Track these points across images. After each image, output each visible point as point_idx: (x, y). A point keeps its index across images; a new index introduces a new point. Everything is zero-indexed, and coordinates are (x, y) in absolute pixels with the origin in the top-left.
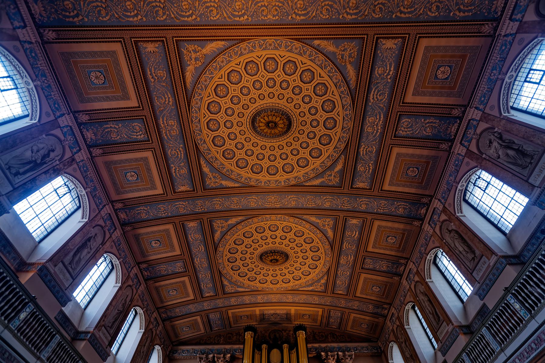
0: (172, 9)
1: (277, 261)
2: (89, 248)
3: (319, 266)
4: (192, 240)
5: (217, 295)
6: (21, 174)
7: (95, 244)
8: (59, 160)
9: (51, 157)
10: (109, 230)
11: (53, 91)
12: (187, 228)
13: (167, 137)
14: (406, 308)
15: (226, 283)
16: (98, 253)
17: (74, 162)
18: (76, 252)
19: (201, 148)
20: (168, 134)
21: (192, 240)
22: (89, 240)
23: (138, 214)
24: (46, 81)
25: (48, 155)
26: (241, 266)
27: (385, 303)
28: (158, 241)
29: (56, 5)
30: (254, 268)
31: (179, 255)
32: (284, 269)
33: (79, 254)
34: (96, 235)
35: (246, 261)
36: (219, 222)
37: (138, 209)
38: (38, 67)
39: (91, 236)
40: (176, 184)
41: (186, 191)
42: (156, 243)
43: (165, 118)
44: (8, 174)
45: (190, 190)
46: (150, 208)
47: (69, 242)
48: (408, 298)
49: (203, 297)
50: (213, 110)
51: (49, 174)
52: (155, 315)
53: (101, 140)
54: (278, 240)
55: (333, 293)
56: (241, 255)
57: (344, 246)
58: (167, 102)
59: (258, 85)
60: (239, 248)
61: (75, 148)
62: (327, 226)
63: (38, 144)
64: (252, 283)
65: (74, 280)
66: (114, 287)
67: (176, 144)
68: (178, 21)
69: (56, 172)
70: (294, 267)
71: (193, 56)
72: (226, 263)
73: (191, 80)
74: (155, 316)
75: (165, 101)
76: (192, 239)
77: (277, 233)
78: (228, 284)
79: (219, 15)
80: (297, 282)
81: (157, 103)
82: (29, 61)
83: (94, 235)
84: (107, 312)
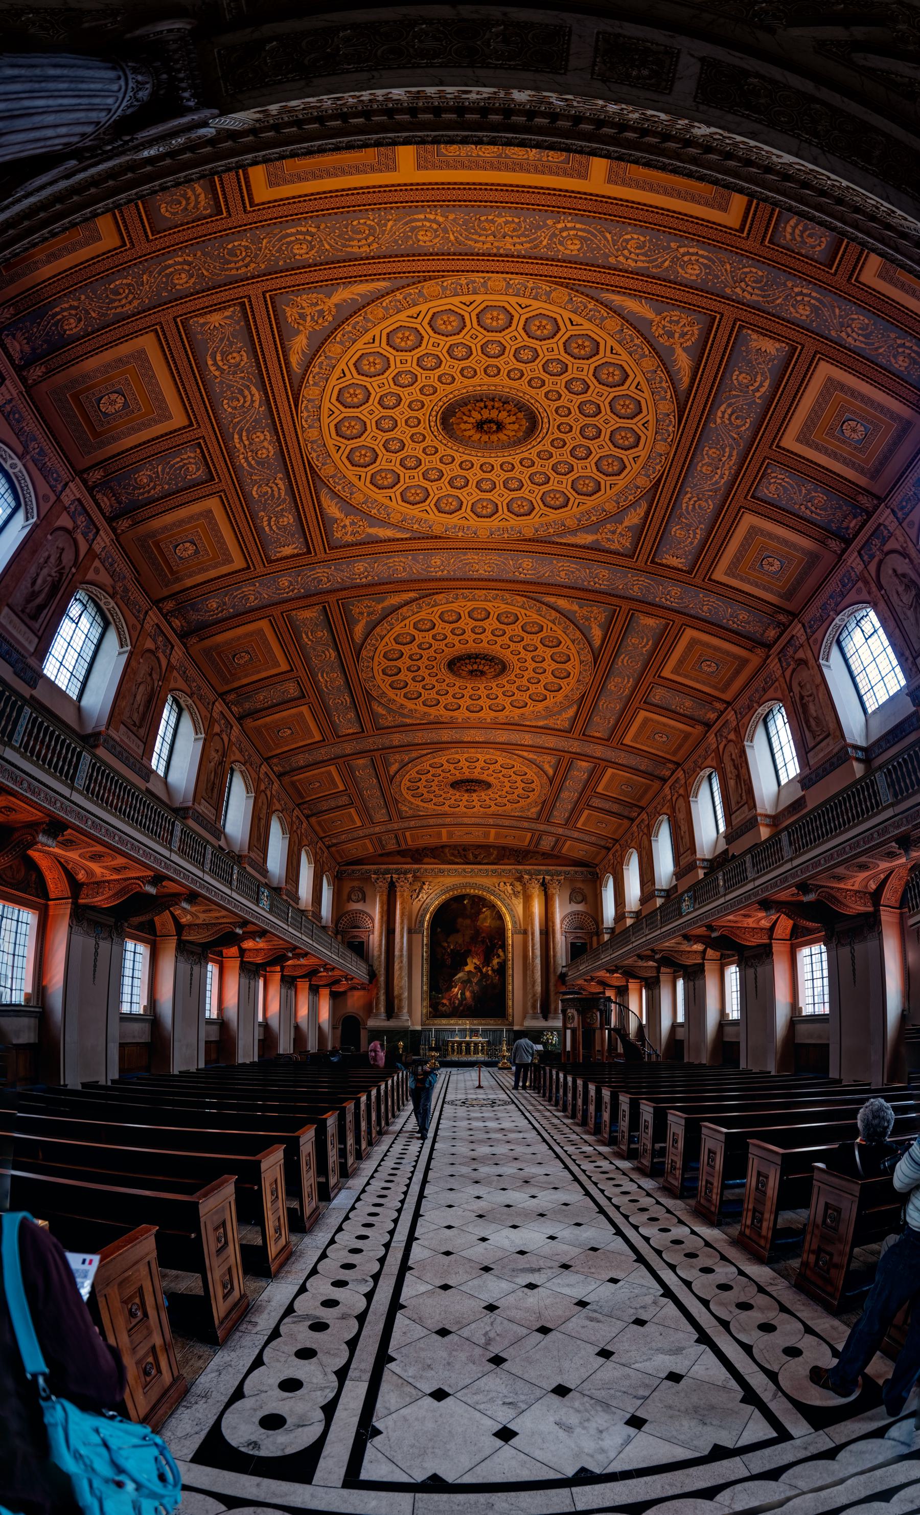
48: (709, 762)
49: (339, 737)
59: (460, 352)
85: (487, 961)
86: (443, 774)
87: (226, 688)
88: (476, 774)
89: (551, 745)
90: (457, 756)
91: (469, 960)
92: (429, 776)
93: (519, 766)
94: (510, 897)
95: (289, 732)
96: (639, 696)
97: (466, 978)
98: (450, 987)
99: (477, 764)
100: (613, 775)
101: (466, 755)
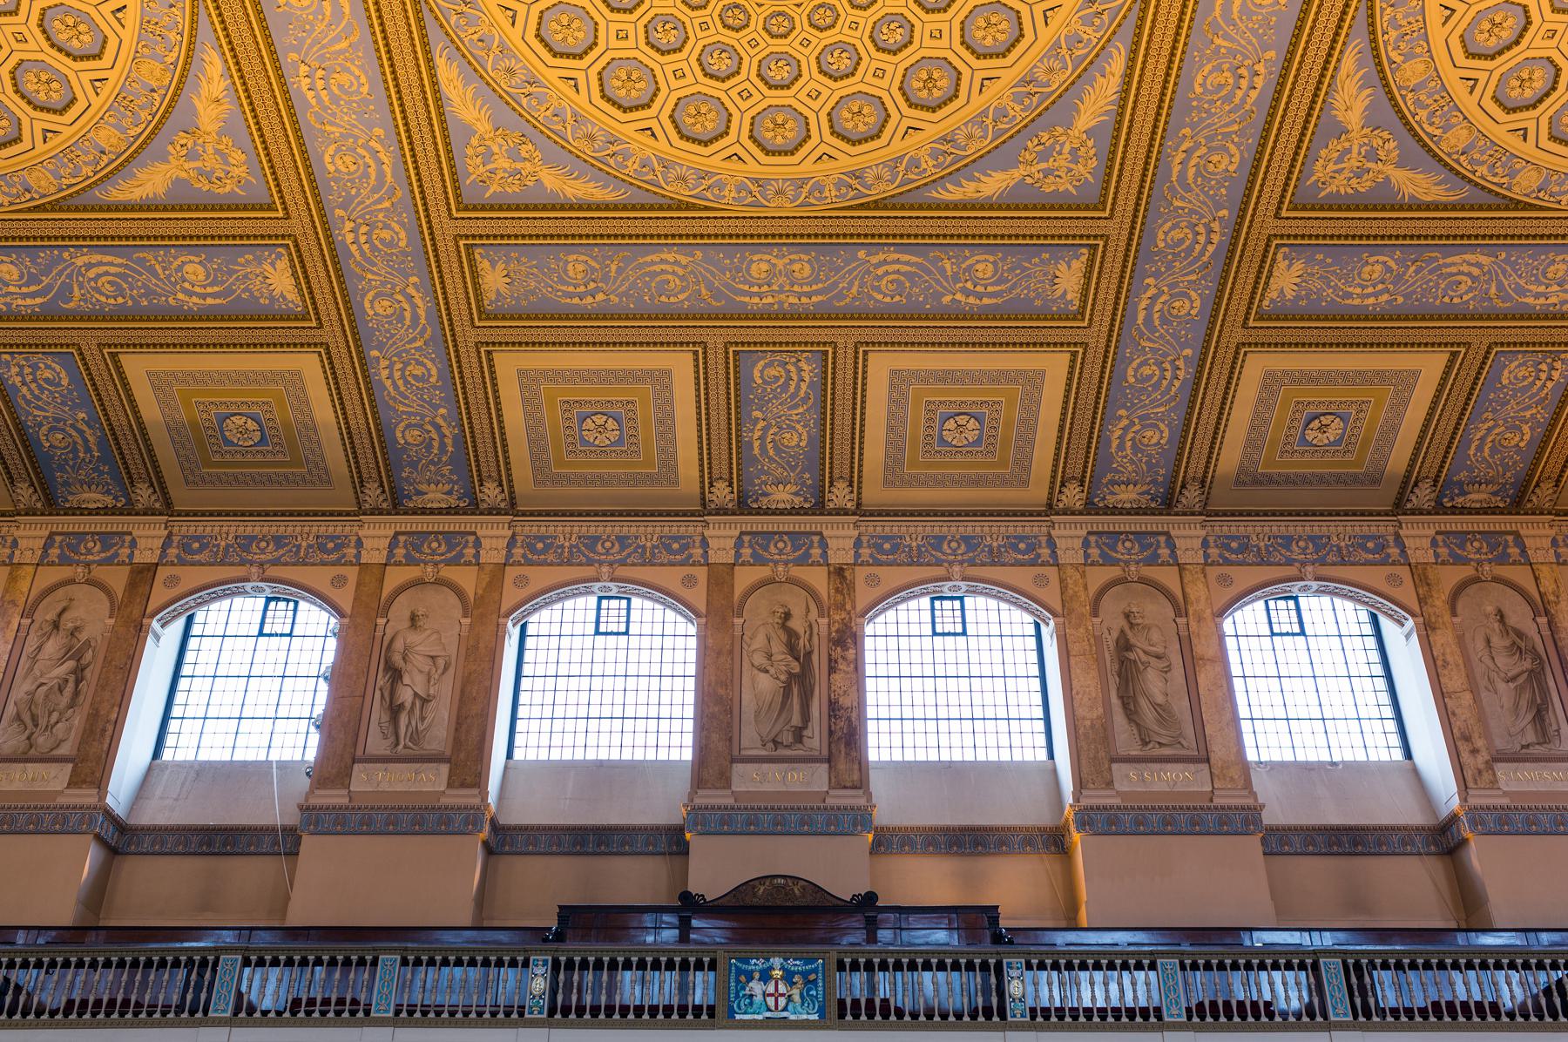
0: (368, 202)
2: (1153, 661)
6: (805, 728)
7: (1155, 636)
8: (821, 615)
9: (802, 633)
10: (1153, 561)
11: (637, 538)
12: (1303, 303)
13: (817, 293)
16: (1195, 641)
17: (847, 574)
18: (1125, 706)
19: (875, 193)
20: (806, 289)
21: (1385, 297)
22: (1124, 645)
23: (1142, 451)
24: (608, 544)
25: (792, 635)
28: (1316, 417)
29: (421, 460)
31: (1451, 362)
33: (1143, 702)
34: (1127, 616)
36: (1320, 171)
37: (1115, 444)
38: (571, 546)
39: (1115, 635)
40: (1038, 303)
41: (1088, 276)
42: (1323, 428)
43: (741, 286)
44: (788, 752)
45: (1084, 259)
46: (1128, 409)
47: (1073, 711)
50: (710, 126)
51: (840, 661)
53: (802, 471)
58: (680, 272)
61: (811, 546)
63: (752, 648)
65: (1208, 761)
66: (1408, 636)
67: (850, 272)
68: (399, 194)
69: (847, 640)
71: (506, 165)
73: (592, 184)
75: (674, 273)
79: (348, 64)
81: (681, 300)
82: (551, 564)
83: (1123, 623)
84: (1458, 724)
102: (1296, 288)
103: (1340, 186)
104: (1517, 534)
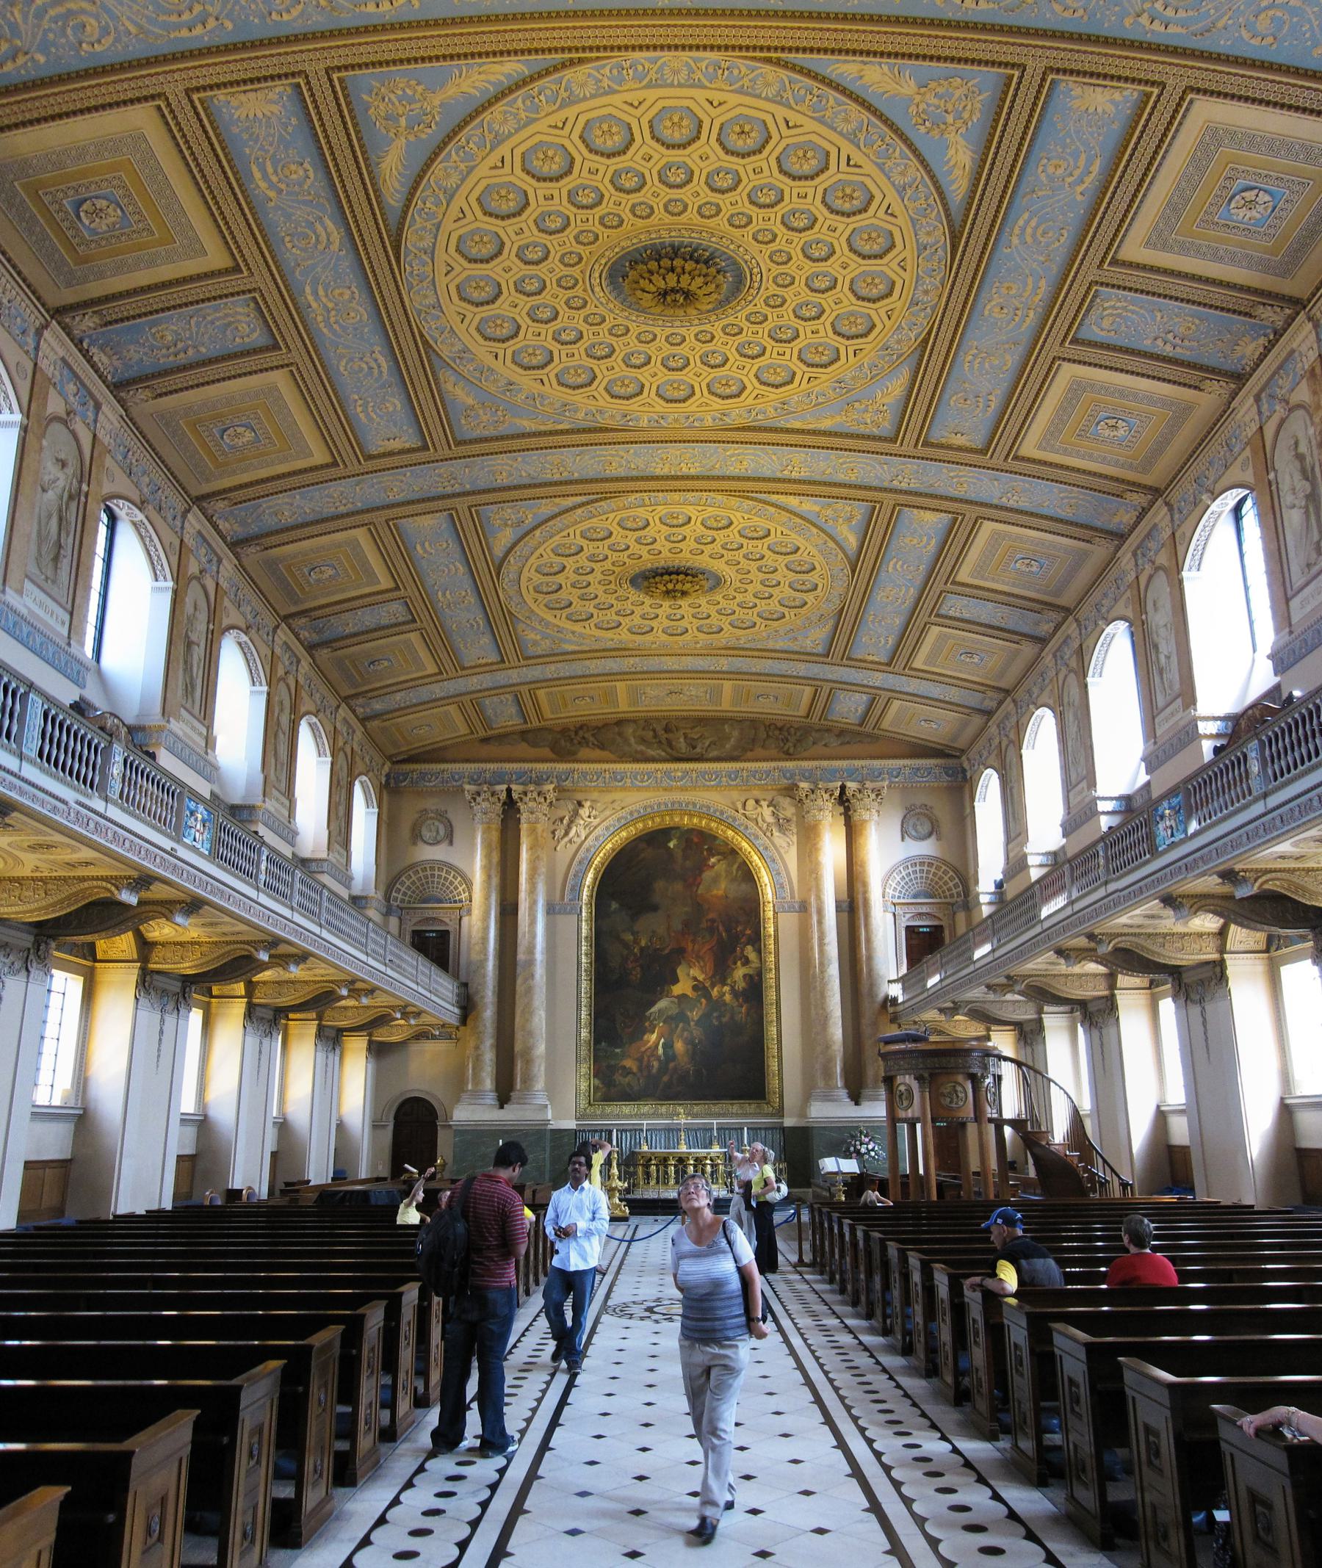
1: (688, 295)
3: (879, 326)
4: (272, 194)
5: (425, 448)
14: (1214, 507)
15: (460, 394)
26: (524, 321)
27: (1134, 484)
30: (584, 327)
32: (718, 333)
35: (545, 297)
48: (1235, 473)
49: (370, 457)
52: (195, 521)
54: (697, 194)
55: (926, 444)
56: (520, 270)
57: (1017, 231)
60: (507, 230)
62: (950, 119)
64: (578, 397)
70: (768, 325)
72: (453, 307)
74: (198, 527)
76: (272, 186)
77: (690, 157)
78: (470, 401)
80: (773, 394)
85: (721, 972)
86: (614, 556)
87: (69, 297)
88: (686, 558)
89: (852, 478)
90: (641, 512)
91: (681, 971)
92: (582, 560)
93: (781, 530)
94: (767, 832)
95: (249, 436)
96: (1061, 325)
97: (674, 1011)
98: (640, 1032)
99: (686, 530)
100: (995, 538)
101: (662, 510)
102: (251, 116)
103: (377, 110)
104: (98, 407)
